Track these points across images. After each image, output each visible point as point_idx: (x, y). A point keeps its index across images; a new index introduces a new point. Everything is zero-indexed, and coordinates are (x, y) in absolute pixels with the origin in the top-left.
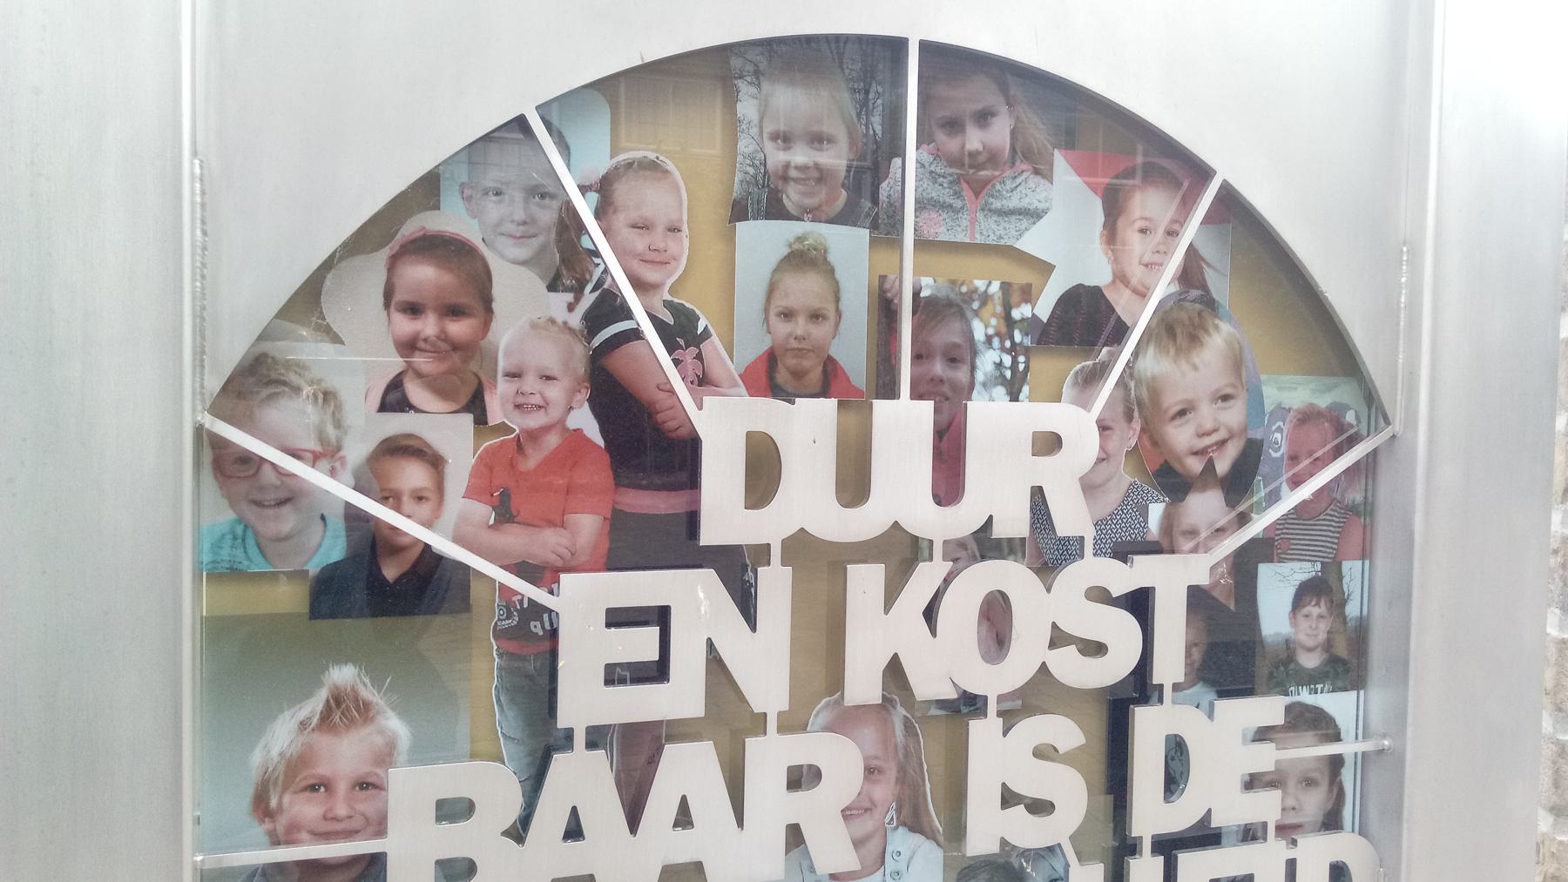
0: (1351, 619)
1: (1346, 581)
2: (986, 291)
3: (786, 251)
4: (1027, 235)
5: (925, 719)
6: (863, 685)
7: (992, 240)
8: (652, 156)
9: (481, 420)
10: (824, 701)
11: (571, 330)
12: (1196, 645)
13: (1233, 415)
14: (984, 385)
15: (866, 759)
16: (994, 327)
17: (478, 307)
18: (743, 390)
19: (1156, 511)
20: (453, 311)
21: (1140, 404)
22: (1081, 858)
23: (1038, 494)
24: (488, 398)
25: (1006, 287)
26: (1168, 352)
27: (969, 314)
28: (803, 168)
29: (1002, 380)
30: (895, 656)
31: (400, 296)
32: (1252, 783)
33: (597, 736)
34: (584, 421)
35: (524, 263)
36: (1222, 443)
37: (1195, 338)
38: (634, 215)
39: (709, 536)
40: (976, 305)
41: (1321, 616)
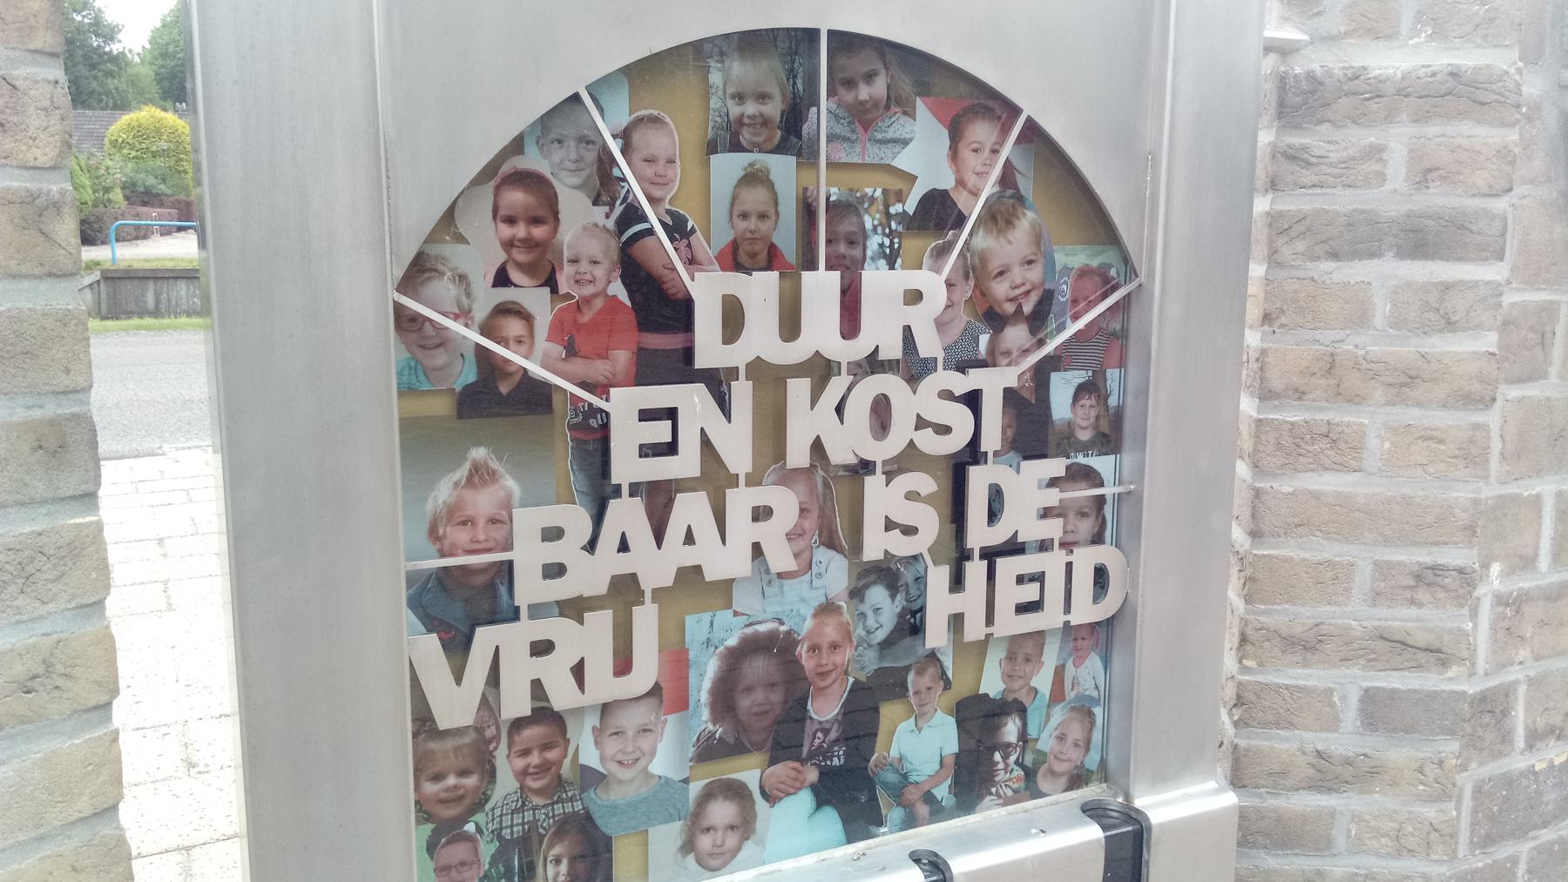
1: (1108, 382)
2: (872, 196)
3: (743, 173)
4: (899, 156)
5: (835, 478)
6: (798, 455)
7: (876, 161)
8: (655, 113)
9: (554, 290)
10: (772, 468)
11: (608, 230)
12: (1009, 427)
13: (1035, 274)
14: (872, 259)
15: (800, 503)
16: (878, 220)
17: (551, 220)
18: (717, 267)
19: (984, 339)
20: (535, 221)
21: (974, 269)
22: (935, 563)
24: (558, 276)
25: (885, 192)
26: (992, 232)
27: (862, 211)
28: (752, 117)
29: (885, 256)
31: (502, 212)
32: (1046, 513)
33: (635, 489)
34: (618, 290)
35: (578, 188)
36: (1028, 292)
37: (1009, 223)
38: (644, 153)
39: (701, 362)
40: (866, 205)
41: (1092, 406)
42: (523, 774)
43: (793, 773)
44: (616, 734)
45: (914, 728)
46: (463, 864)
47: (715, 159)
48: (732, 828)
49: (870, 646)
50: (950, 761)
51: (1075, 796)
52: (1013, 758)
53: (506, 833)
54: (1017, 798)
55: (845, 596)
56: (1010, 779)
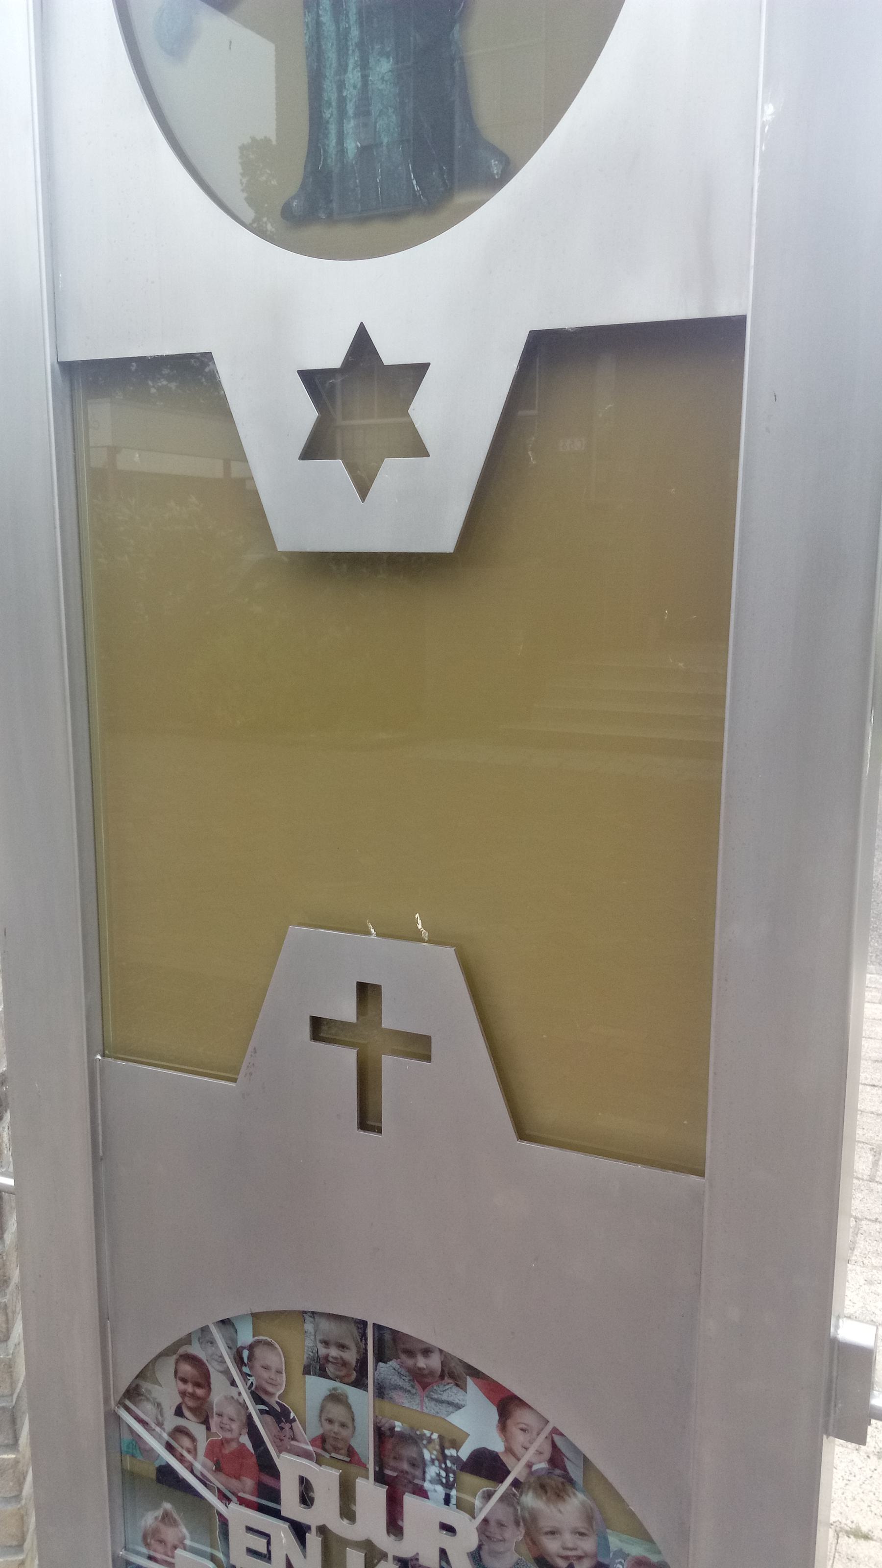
3: (329, 1393)
4: (453, 1415)
8: (269, 1340)
9: (208, 1429)
21: (524, 1520)
25: (440, 1437)
27: (421, 1446)
28: (336, 1358)
31: (179, 1375)
34: (245, 1440)
35: (221, 1372)
40: (425, 1442)
47: (307, 1377)
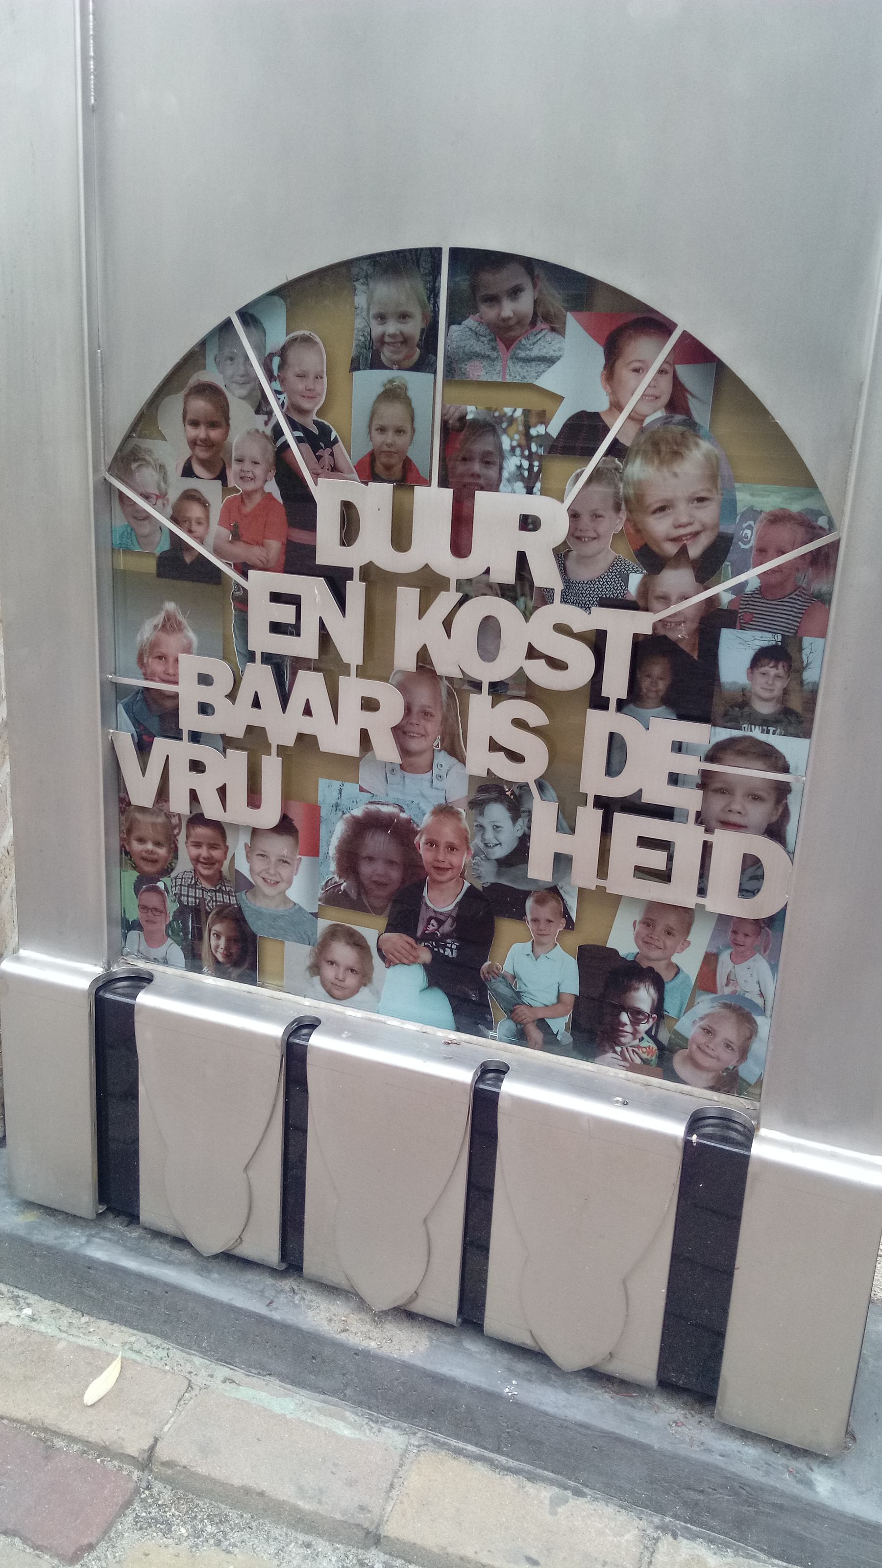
0: (807, 684)
2: (512, 416)
3: (382, 389)
4: (545, 376)
7: (518, 379)
8: (307, 333)
9: (225, 483)
11: (266, 437)
12: (661, 679)
13: (707, 514)
14: (509, 480)
16: (517, 440)
17: (224, 424)
18: (356, 476)
19: (635, 580)
20: (213, 425)
23: (522, 558)
24: (228, 471)
25: (526, 413)
26: (653, 462)
27: (499, 431)
28: (393, 336)
29: (522, 478)
30: (425, 645)
31: (188, 417)
32: (674, 779)
33: (267, 658)
34: (272, 488)
36: (696, 534)
37: (677, 455)
38: (297, 370)
40: (504, 425)
41: (778, 676)
42: (196, 860)
43: (408, 947)
44: (262, 855)
45: (531, 953)
46: (156, 909)
47: (356, 374)
48: (352, 970)
49: (487, 859)
50: (570, 1001)
51: (716, 1099)
52: (643, 1027)
53: (184, 899)
54: (643, 1068)
55: (465, 804)
56: (638, 1047)
